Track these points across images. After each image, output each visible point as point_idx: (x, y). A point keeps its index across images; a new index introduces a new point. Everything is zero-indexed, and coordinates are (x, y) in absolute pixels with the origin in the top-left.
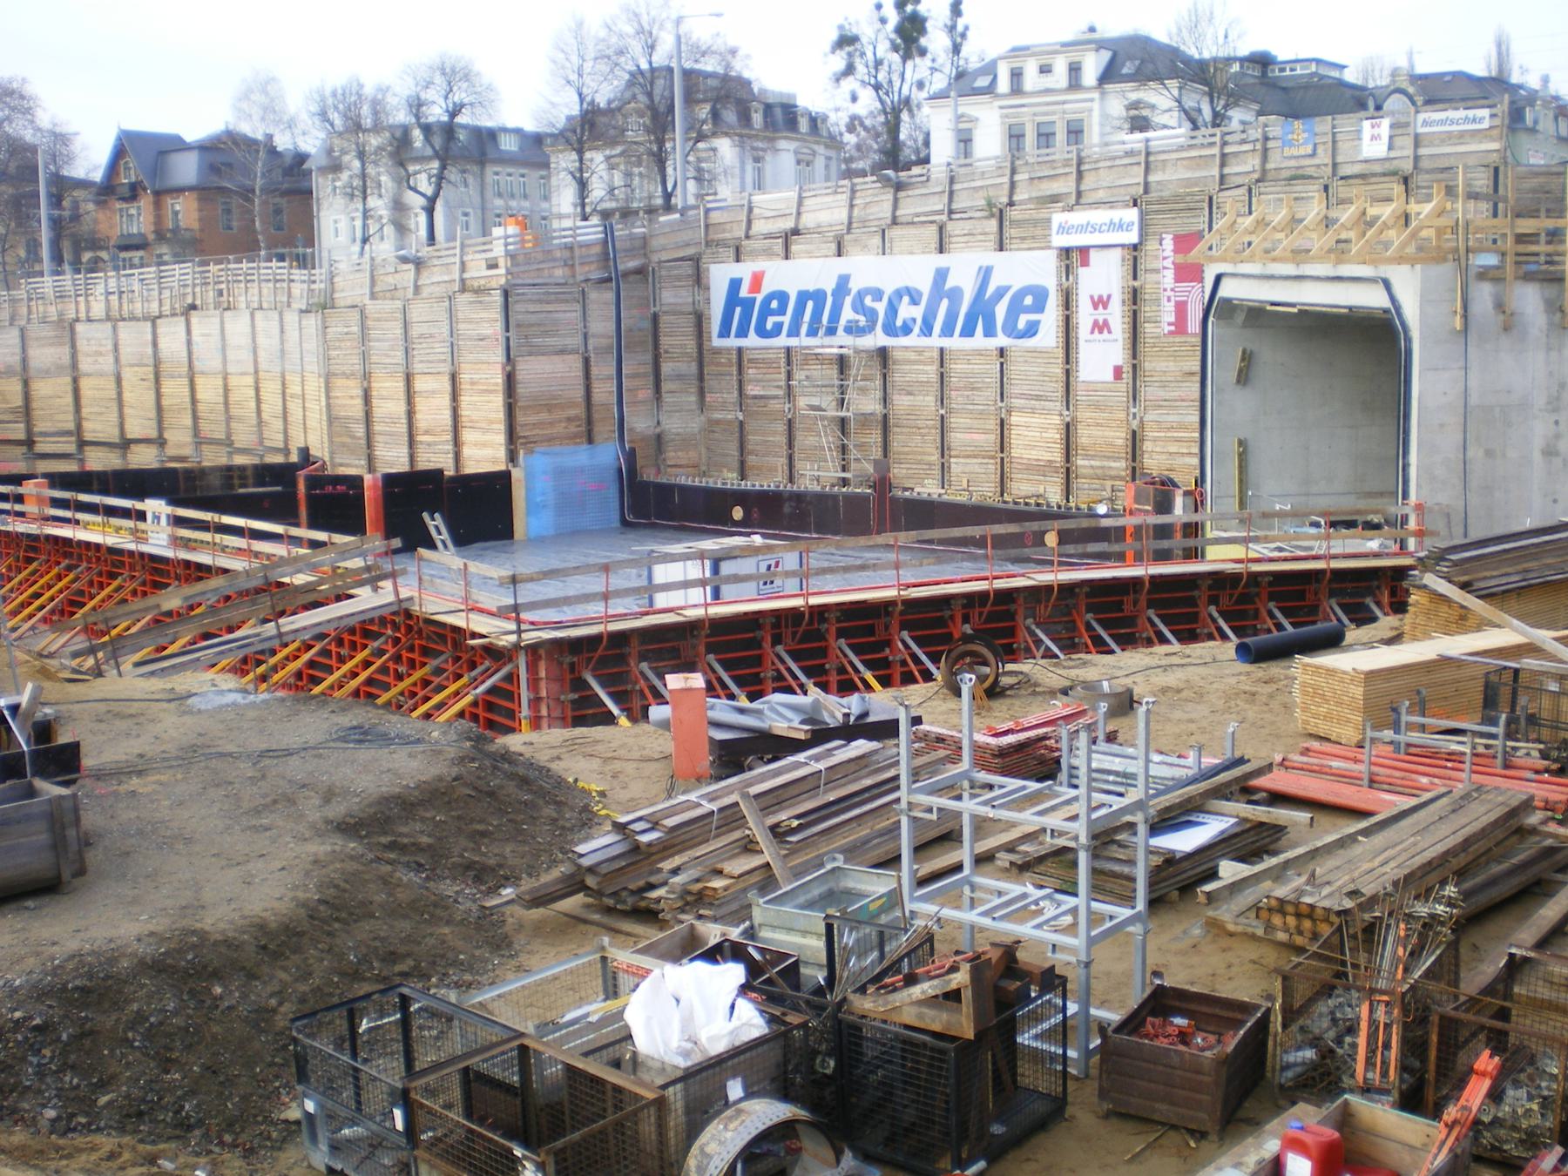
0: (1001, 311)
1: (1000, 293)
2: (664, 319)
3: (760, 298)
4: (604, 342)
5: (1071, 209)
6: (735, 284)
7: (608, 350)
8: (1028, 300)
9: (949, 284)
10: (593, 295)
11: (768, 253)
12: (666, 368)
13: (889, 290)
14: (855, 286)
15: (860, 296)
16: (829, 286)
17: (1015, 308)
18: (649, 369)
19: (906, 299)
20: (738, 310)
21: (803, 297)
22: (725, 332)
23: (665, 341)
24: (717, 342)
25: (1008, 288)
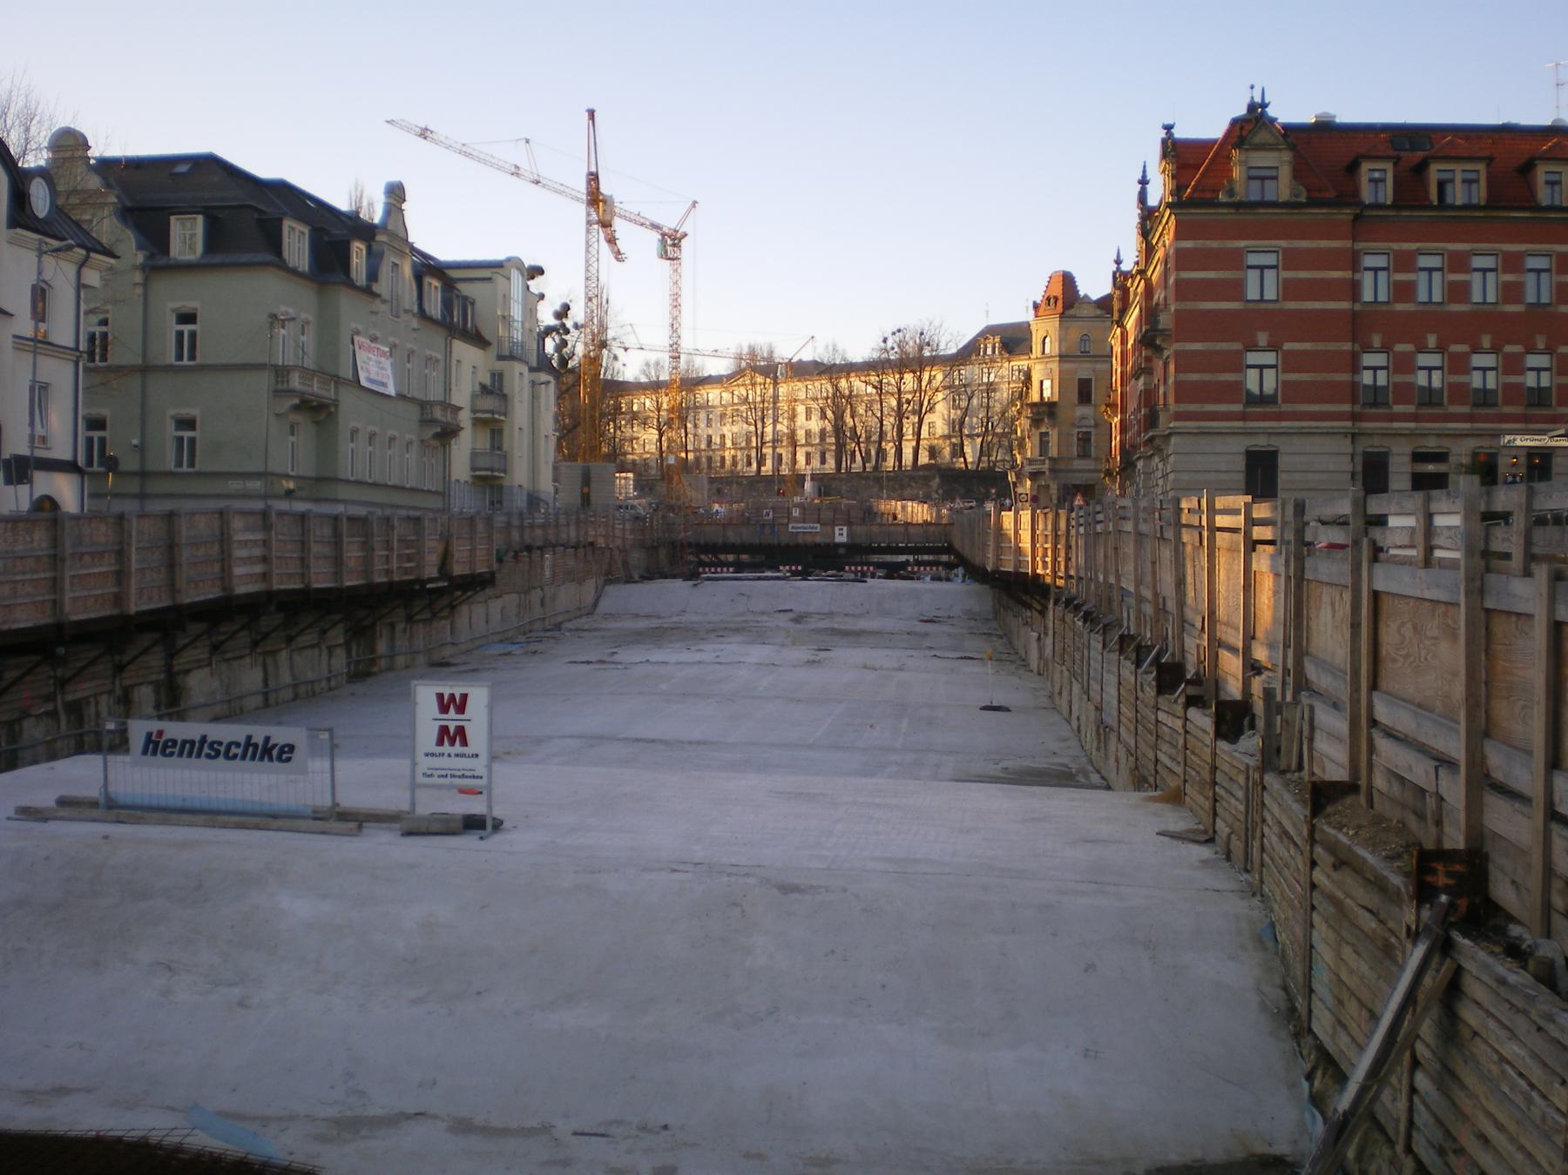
0: (275, 752)
1: (275, 746)
3: (162, 740)
8: (286, 749)
9: (253, 741)
13: (225, 743)
14: (210, 739)
15: (213, 743)
16: (197, 738)
17: (282, 751)
21: (184, 742)
25: (276, 745)
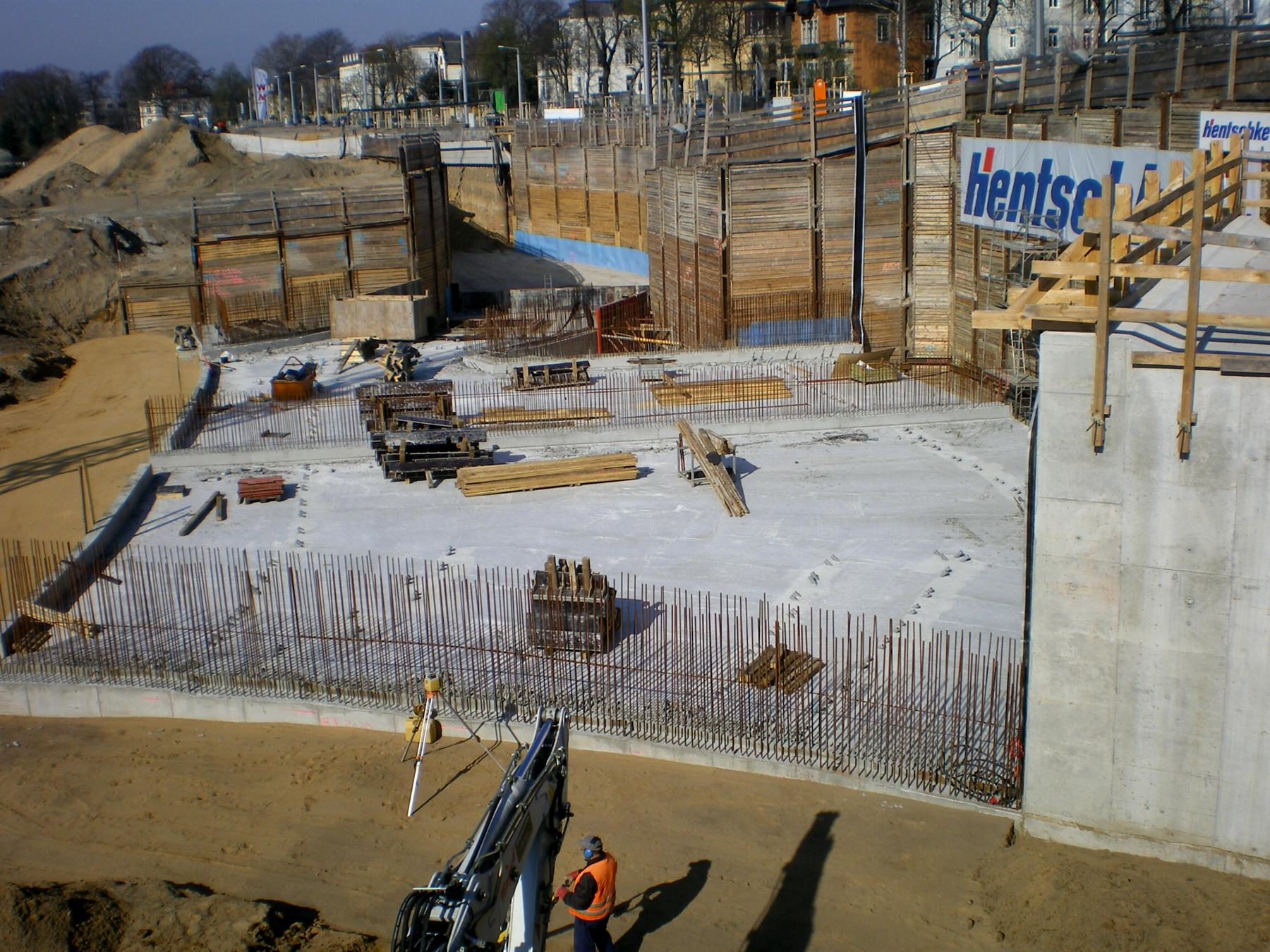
2: (920, 194)
3: (991, 174)
4: (839, 216)
5: (1217, 107)
6: (976, 157)
7: (844, 225)
10: (827, 170)
11: (996, 133)
12: (919, 240)
13: (1078, 183)
14: (1055, 173)
16: (1036, 170)
18: (899, 241)
19: (1090, 193)
20: (977, 185)
22: (967, 211)
23: (920, 214)
24: (964, 218)
